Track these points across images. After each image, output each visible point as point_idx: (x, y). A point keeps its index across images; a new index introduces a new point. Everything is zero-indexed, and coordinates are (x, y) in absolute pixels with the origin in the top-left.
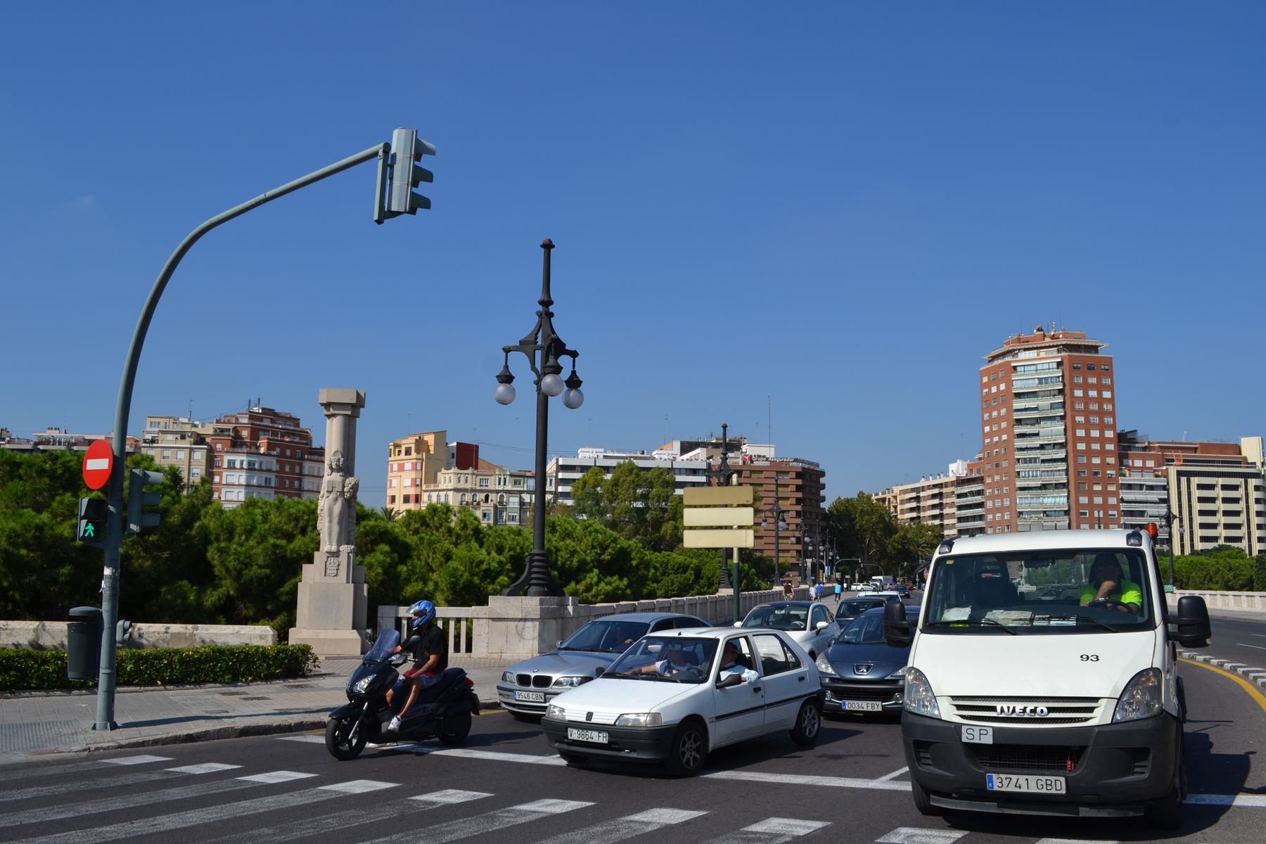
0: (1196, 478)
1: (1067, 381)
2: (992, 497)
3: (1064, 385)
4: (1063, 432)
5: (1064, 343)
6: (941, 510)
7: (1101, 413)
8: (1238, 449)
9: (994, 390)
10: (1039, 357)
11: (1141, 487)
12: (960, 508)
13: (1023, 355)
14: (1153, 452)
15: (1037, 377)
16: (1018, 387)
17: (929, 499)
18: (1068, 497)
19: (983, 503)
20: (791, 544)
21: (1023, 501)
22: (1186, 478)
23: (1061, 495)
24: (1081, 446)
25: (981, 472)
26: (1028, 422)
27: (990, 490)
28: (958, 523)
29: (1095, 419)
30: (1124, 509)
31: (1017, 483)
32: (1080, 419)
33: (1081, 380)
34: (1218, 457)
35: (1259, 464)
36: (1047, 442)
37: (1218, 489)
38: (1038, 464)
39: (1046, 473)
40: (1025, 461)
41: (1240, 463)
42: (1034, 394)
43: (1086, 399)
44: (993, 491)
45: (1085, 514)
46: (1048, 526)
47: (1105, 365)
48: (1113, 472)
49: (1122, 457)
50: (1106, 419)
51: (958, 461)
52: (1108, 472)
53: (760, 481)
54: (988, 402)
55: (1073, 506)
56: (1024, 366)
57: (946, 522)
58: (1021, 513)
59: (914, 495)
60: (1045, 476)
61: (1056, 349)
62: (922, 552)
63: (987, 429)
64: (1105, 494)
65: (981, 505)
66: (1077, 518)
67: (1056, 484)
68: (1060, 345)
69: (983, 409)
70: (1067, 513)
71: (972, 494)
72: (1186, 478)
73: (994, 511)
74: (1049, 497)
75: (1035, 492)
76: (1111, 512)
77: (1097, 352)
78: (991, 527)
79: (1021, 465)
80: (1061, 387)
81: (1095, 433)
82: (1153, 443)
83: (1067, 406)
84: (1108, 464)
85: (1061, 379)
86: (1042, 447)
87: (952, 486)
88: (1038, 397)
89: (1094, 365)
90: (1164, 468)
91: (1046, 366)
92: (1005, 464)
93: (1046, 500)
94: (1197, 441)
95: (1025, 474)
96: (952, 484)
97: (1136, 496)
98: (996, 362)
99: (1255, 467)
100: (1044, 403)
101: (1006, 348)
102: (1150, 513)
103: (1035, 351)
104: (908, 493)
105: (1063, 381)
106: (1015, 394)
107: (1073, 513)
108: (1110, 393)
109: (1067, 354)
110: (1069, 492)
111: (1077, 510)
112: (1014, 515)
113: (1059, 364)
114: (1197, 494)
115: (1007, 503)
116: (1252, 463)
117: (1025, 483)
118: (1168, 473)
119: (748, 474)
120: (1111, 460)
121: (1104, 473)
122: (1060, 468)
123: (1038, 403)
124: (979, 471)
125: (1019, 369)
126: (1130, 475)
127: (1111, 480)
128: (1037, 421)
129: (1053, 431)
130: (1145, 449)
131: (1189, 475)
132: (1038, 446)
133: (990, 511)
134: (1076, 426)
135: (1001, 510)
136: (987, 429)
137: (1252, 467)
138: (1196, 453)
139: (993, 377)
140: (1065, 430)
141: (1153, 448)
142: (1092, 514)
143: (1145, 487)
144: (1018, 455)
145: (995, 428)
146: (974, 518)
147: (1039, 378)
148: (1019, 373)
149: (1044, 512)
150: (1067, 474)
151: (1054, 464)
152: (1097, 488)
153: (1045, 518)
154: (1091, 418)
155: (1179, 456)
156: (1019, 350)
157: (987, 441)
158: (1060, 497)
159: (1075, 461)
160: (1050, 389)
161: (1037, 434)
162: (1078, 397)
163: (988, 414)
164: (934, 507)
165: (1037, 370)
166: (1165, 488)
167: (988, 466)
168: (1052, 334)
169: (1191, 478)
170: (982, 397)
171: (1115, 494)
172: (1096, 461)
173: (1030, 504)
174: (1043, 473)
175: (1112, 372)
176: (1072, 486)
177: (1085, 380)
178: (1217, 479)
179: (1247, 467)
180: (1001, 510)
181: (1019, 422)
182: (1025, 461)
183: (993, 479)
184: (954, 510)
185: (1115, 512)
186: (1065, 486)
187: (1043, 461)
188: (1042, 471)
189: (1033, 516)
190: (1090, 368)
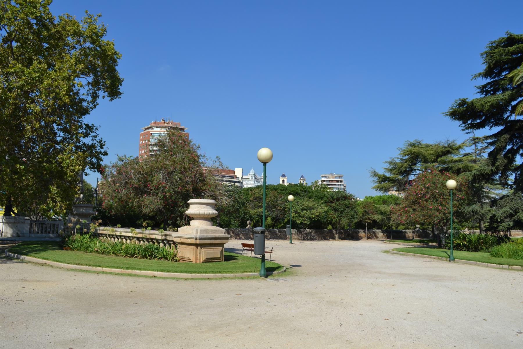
5: (171, 126)
8: (234, 172)
13: (155, 129)
35: (240, 178)
41: (233, 177)
69: (140, 149)
77: (184, 131)
98: (147, 131)
101: (150, 126)
103: (160, 128)
116: (238, 178)
125: (153, 134)
139: (144, 137)
170: (140, 144)
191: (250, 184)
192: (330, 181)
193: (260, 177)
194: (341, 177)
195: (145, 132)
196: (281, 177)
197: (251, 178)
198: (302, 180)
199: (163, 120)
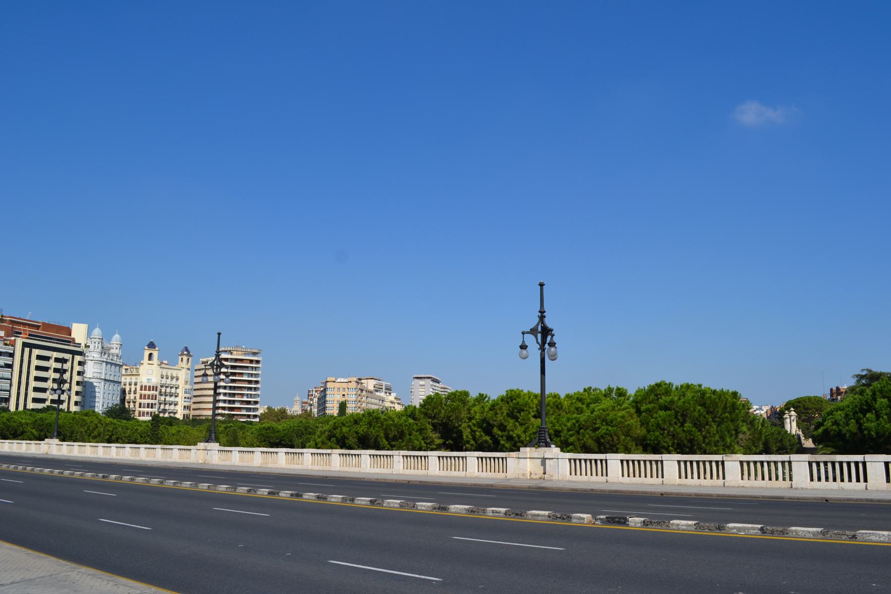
0: (37, 350)
8: (69, 331)
14: (4, 324)
22: (29, 349)
35: (83, 345)
37: (52, 361)
41: (70, 342)
72: (29, 349)
82: (5, 317)
90: (13, 338)
94: (40, 321)
99: (80, 347)
114: (35, 362)
116: (78, 344)
118: (15, 343)
131: (32, 346)
137: (78, 347)
138: (38, 330)
141: (5, 321)
155: (26, 330)
166: (12, 355)
169: (33, 349)
178: (52, 352)
179: (75, 346)
191: (92, 358)
192: (236, 360)
193: (109, 346)
194: (257, 353)
197: (95, 347)
198: (186, 355)
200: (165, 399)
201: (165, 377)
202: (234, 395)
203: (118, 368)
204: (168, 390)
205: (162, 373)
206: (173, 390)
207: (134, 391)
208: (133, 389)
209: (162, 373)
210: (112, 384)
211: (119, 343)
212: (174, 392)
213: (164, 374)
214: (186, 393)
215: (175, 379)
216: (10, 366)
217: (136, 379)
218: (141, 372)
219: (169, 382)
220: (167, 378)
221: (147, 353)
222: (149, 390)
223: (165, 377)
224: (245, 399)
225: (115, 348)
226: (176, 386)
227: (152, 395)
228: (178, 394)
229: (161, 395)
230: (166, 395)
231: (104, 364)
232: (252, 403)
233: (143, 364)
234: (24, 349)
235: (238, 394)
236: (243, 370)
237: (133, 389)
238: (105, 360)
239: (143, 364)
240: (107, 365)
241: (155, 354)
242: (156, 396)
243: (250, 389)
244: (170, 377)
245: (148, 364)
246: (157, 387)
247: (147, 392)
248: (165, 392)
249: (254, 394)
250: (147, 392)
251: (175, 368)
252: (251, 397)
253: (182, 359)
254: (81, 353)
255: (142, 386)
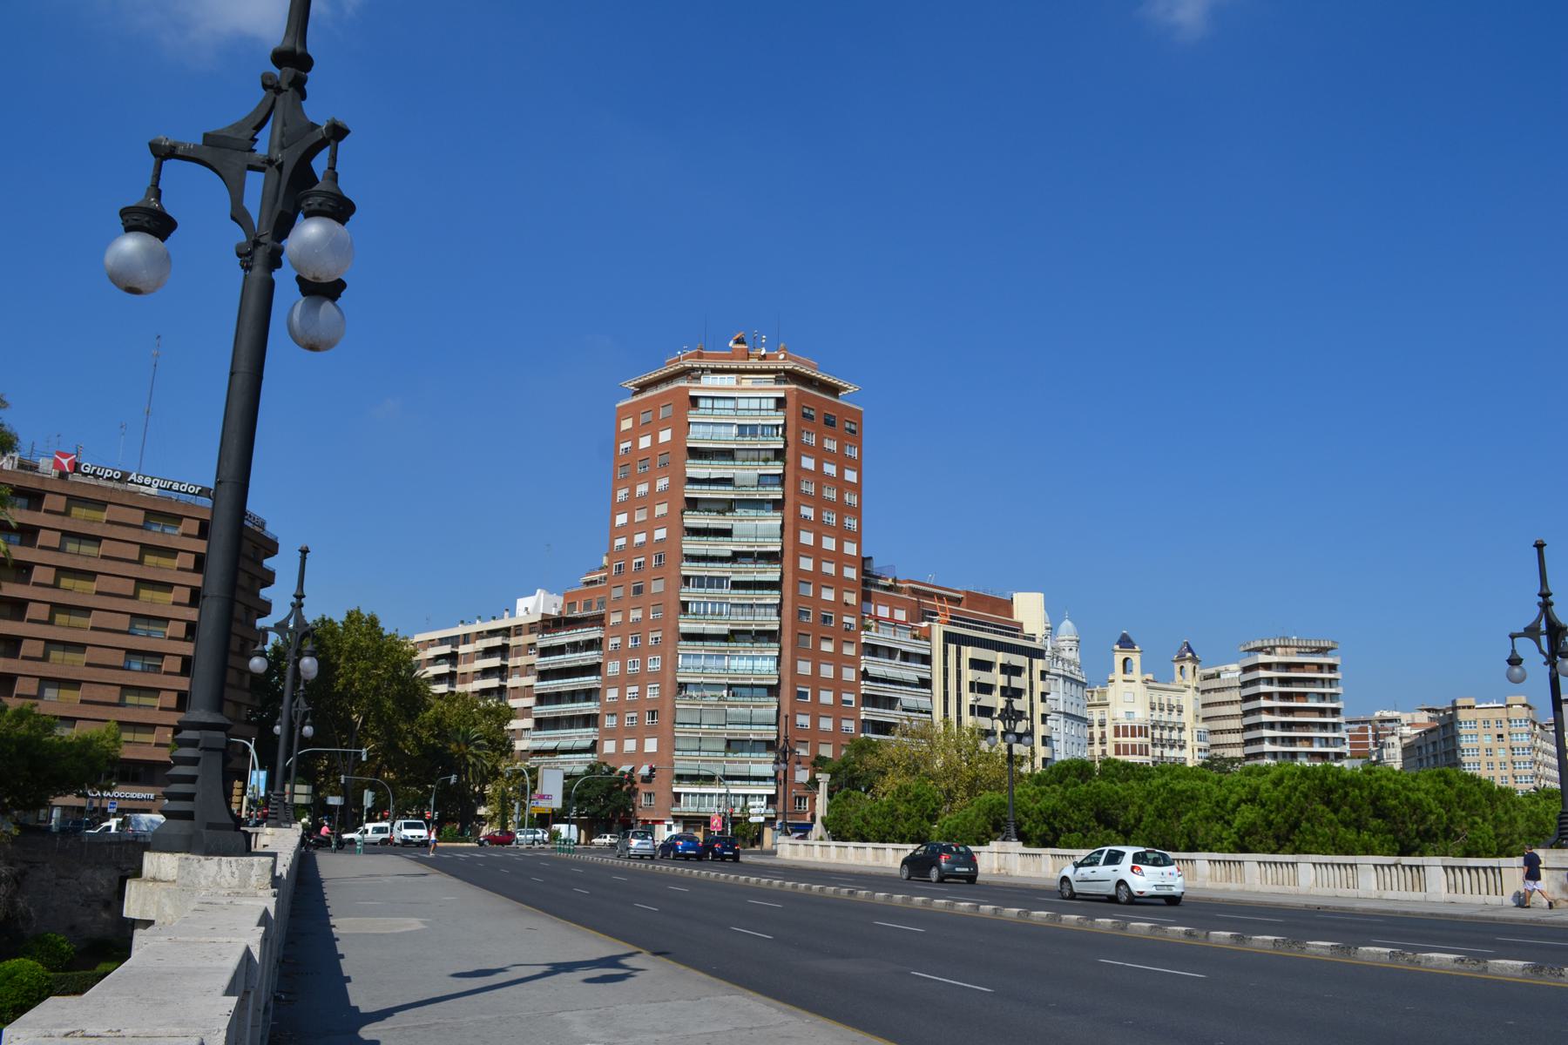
1: (791, 436)
2: (619, 653)
3: (786, 444)
4: (778, 532)
6: (502, 679)
7: (841, 508)
9: (645, 442)
10: (738, 387)
11: (891, 653)
12: (544, 675)
13: (708, 380)
15: (736, 421)
16: (698, 436)
17: (478, 658)
18: (779, 658)
19: (599, 664)
20: (161, 709)
21: (690, 662)
23: (767, 654)
24: (807, 564)
25: (595, 605)
26: (712, 506)
27: (618, 641)
28: (537, 705)
29: (830, 516)
30: (868, 692)
31: (680, 625)
32: (807, 512)
33: (812, 440)
34: (991, 619)
36: (745, 549)
37: (996, 670)
38: (725, 591)
39: (739, 610)
40: (701, 582)
42: (728, 454)
43: (818, 476)
44: (625, 642)
45: (804, 695)
46: (736, 716)
47: (851, 422)
48: (852, 621)
49: (866, 597)
50: (847, 521)
51: (539, 591)
52: (846, 619)
53: (96, 530)
54: (632, 467)
55: (787, 679)
56: (713, 398)
57: (513, 703)
58: (683, 686)
59: (446, 649)
60: (737, 615)
61: (774, 376)
62: (475, 756)
63: (621, 519)
64: (838, 660)
65: (594, 669)
66: (792, 701)
67: (757, 632)
68: (780, 371)
70: (773, 690)
71: (575, 647)
73: (622, 681)
74: (741, 658)
75: (716, 645)
76: (846, 697)
77: (837, 396)
78: (612, 715)
79: (692, 590)
80: (782, 447)
81: (829, 544)
83: (787, 483)
84: (846, 604)
85: (780, 430)
86: (736, 557)
87: (531, 633)
88: (733, 459)
89: (835, 417)
90: (925, 624)
91: (755, 404)
92: (657, 587)
93: (735, 663)
95: (698, 608)
96: (532, 628)
97: (886, 669)
100: (745, 472)
102: (905, 704)
103: (734, 376)
104: (433, 646)
105: (784, 435)
106: (690, 449)
107: (786, 690)
108: (855, 474)
109: (794, 386)
110: (781, 650)
111: (794, 686)
112: (670, 689)
113: (780, 403)
114: (969, 675)
115: (654, 665)
117: (699, 626)
118: (930, 634)
119: (59, 503)
120: (851, 598)
121: (840, 622)
122: (768, 601)
123: (734, 471)
124: (588, 606)
125: (702, 403)
126: (877, 628)
127: (847, 636)
128: (729, 506)
129: (760, 529)
130: (889, 588)
132: (729, 554)
133: (612, 682)
134: (800, 522)
135: (640, 679)
136: (621, 519)
138: (959, 606)
139: (643, 419)
140: (782, 527)
141: (899, 590)
142: (816, 696)
143: (899, 655)
144: (689, 569)
145: (640, 516)
146: (573, 696)
147: (739, 426)
148: (701, 411)
149: (730, 687)
150: (779, 614)
151: (757, 592)
152: (827, 647)
153: (731, 698)
154: (825, 514)
155: (943, 609)
156: (703, 370)
157: (620, 542)
158: (765, 658)
159: (796, 590)
160: (759, 447)
161: (727, 533)
162: (806, 470)
163: (626, 491)
164: (486, 673)
165: (736, 409)
166: (926, 660)
167: (617, 593)
168: (763, 352)
169: (962, 647)
171: (853, 662)
172: (828, 595)
173: (704, 668)
174: (733, 610)
175: (861, 437)
176: (787, 638)
177: (820, 442)
180: (640, 679)
181: (693, 504)
182: (701, 582)
183: (626, 616)
184: (531, 680)
185: (851, 697)
186: (771, 636)
187: (736, 585)
188: (732, 605)
189: (707, 693)
190: (829, 422)
192: (1288, 666)
195: (635, 399)
196: (1117, 647)
199: (738, 341)
200: (1162, 752)
201: (1157, 707)
202: (1292, 741)
203: (1080, 688)
204: (1166, 734)
205: (1151, 698)
206: (1175, 735)
207: (1101, 739)
208: (1097, 735)
209: (1151, 698)
210: (1076, 723)
211: (1074, 638)
212: (1177, 738)
213: (1156, 700)
214: (1199, 740)
215: (1175, 710)
216: (925, 683)
217: (1103, 713)
218: (1110, 697)
219: (1165, 717)
220: (1170, 710)
221: (1119, 658)
222: (1133, 735)
223: (1157, 707)
224: (1317, 748)
225: (1067, 649)
226: (1180, 726)
227: (1140, 746)
228: (1185, 741)
229: (1154, 745)
230: (1163, 746)
231: (1061, 680)
232: (1332, 757)
233: (1113, 681)
234: (947, 646)
235: (1301, 738)
236: (1305, 687)
237: (1097, 735)
238: (1061, 672)
239: (1113, 681)
240: (1065, 682)
241: (1136, 659)
242: (1147, 746)
243: (1324, 726)
244: (1166, 708)
245: (1124, 681)
246: (1146, 728)
247: (1129, 740)
248: (1161, 739)
249: (1334, 738)
250: (1129, 740)
251: (1174, 687)
252: (1327, 745)
253: (1182, 667)
254: (1040, 654)
255: (1117, 729)
